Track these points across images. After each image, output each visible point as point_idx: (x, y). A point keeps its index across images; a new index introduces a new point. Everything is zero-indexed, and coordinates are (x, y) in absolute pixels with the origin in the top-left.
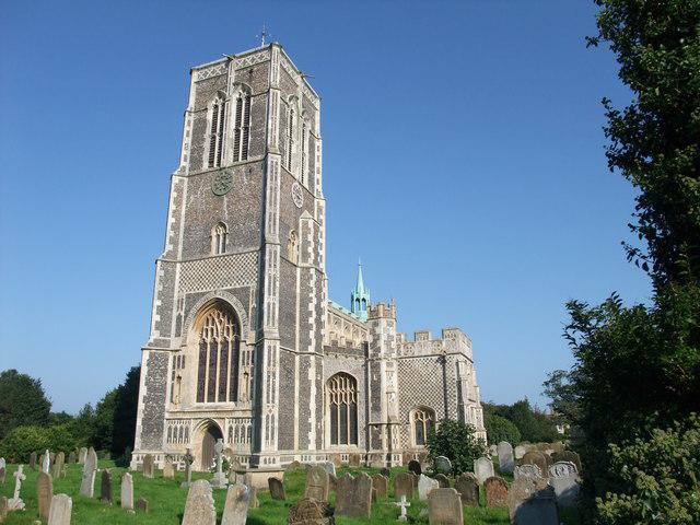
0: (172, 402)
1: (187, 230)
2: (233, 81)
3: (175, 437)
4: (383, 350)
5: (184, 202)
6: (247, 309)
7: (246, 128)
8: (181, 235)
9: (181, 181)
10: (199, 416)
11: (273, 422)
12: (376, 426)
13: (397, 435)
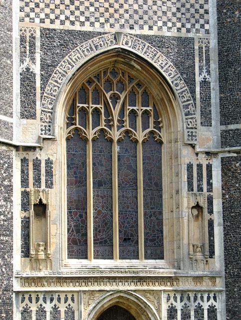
0: (26, 253)
6: (190, 82)
10: (96, 287)
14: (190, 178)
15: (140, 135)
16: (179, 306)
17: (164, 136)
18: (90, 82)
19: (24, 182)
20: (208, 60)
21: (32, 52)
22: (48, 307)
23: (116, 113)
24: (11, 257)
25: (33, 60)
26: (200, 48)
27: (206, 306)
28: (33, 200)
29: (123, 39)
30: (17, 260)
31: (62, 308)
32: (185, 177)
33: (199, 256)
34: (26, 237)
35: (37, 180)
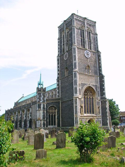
0: (81, 113)
6: (97, 91)
15: (91, 98)
16: (97, 120)
17: (94, 98)
23: (88, 94)
28: (81, 106)
29: (90, 85)
35: (81, 103)
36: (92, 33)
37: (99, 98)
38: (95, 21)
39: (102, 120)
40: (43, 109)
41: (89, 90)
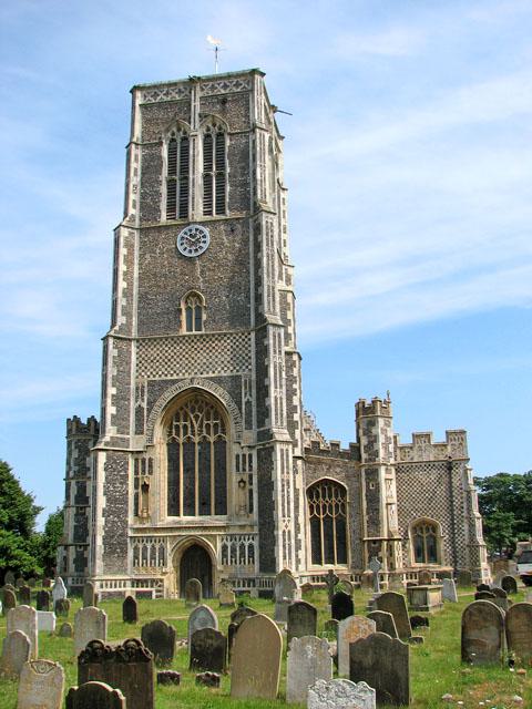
0: (136, 514)
1: (143, 297)
2: (198, 111)
3: (144, 558)
4: (382, 453)
5: (136, 261)
6: (239, 403)
7: (221, 176)
8: (135, 305)
9: (131, 234)
11: (289, 539)
12: (375, 542)
13: (398, 553)
14: (238, 463)
15: (212, 439)
16: (229, 544)
18: (182, 409)
19: (136, 472)
20: (250, 387)
21: (142, 396)
22: (149, 546)
24: (127, 516)
25: (143, 400)
26: (246, 381)
27: (247, 544)
28: (141, 483)
30: (131, 519)
31: (157, 546)
32: (234, 463)
33: (242, 512)
34: (136, 504)
35: (144, 471)
36: (230, 134)
37: (250, 436)
38: (248, 67)
39: (261, 547)
40: (77, 502)
41: (193, 404)
